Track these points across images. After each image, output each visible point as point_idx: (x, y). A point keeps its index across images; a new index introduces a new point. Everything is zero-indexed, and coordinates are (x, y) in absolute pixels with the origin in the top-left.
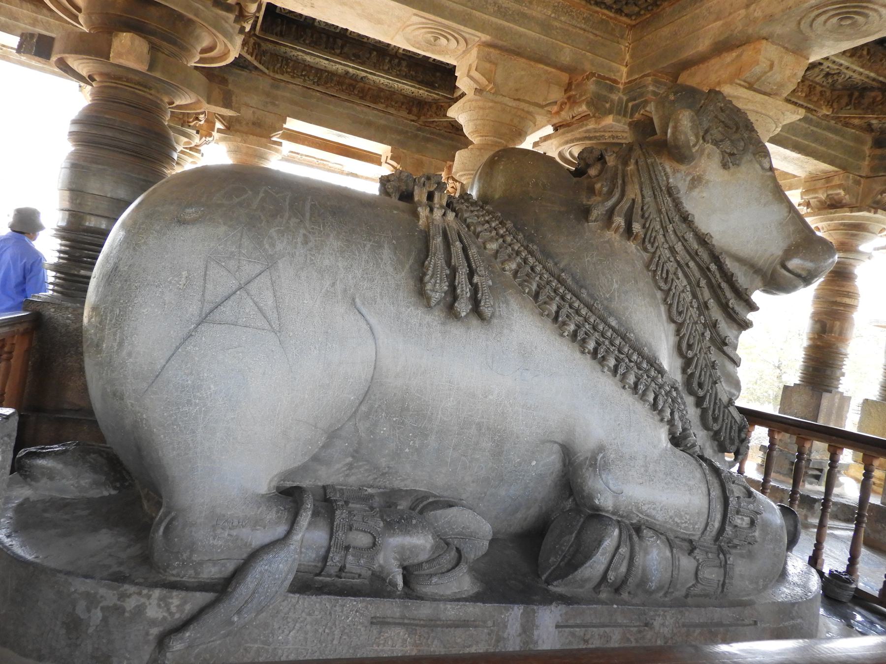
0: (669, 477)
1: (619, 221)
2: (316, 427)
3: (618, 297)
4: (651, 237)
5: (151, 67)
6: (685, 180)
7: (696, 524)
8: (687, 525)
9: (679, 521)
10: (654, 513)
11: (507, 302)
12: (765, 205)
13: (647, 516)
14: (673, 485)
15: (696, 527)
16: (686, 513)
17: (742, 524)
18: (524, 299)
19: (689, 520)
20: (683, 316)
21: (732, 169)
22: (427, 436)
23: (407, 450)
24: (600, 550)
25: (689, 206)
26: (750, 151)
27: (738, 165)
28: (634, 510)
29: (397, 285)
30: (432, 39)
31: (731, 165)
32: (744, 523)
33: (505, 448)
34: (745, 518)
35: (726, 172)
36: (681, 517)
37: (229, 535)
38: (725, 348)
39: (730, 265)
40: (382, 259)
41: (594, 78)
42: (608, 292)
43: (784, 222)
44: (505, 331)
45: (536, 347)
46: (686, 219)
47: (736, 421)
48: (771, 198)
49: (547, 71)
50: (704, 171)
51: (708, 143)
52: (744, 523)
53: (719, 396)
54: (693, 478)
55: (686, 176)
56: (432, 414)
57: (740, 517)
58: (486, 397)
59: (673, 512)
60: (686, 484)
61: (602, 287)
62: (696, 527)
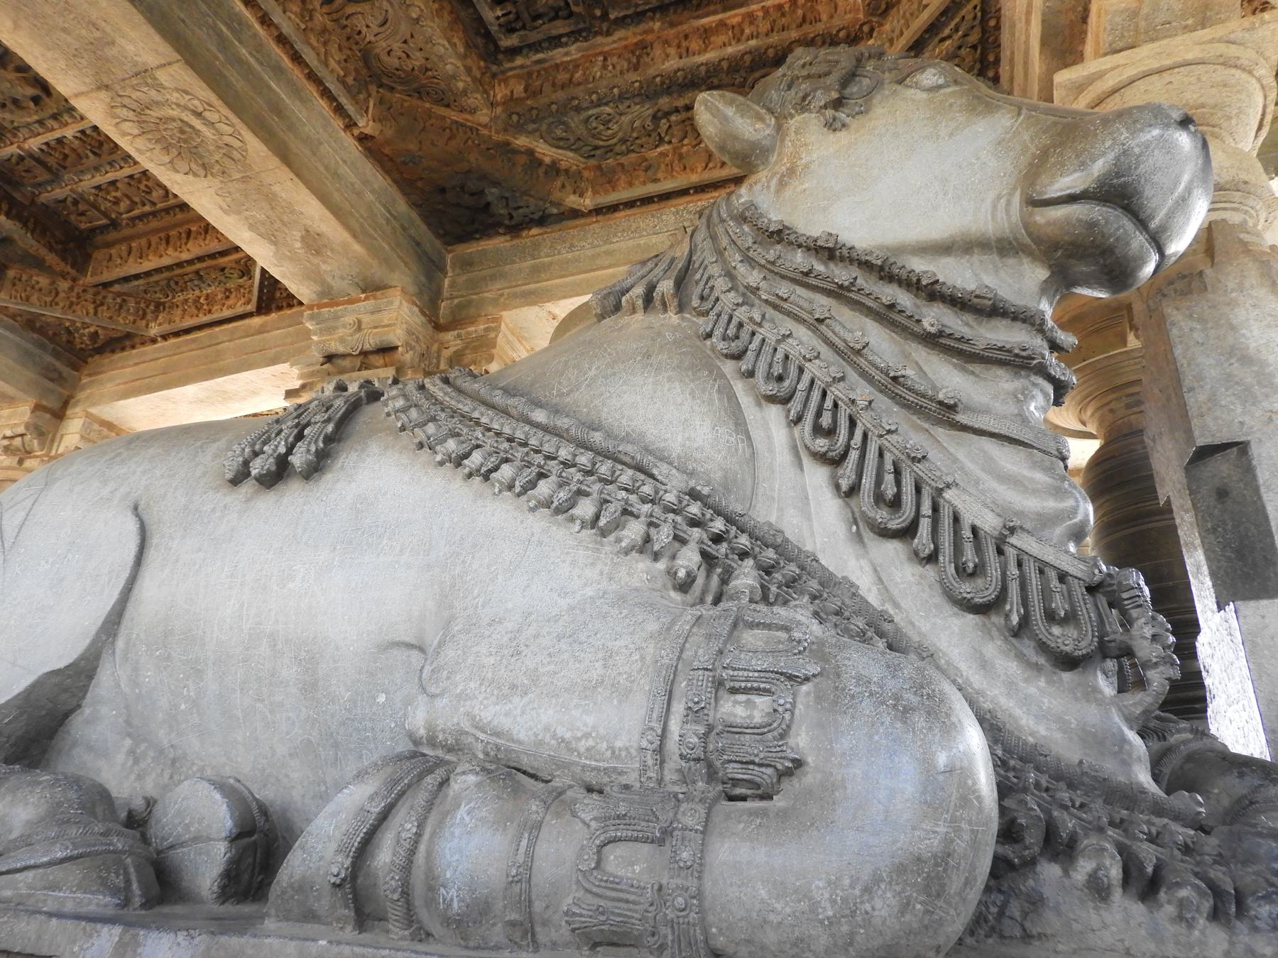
6: (768, 187)
8: (591, 743)
9: (568, 735)
12: (951, 135)
13: (497, 734)
14: (566, 656)
15: (618, 744)
17: (751, 717)
19: (594, 727)
25: (775, 215)
27: (867, 112)
29: (204, 474)
31: (848, 120)
34: (759, 700)
35: (842, 135)
38: (961, 418)
39: (919, 265)
43: (1008, 136)
45: (386, 493)
46: (779, 235)
47: (1063, 577)
51: (792, 116)
53: (968, 519)
56: (204, 633)
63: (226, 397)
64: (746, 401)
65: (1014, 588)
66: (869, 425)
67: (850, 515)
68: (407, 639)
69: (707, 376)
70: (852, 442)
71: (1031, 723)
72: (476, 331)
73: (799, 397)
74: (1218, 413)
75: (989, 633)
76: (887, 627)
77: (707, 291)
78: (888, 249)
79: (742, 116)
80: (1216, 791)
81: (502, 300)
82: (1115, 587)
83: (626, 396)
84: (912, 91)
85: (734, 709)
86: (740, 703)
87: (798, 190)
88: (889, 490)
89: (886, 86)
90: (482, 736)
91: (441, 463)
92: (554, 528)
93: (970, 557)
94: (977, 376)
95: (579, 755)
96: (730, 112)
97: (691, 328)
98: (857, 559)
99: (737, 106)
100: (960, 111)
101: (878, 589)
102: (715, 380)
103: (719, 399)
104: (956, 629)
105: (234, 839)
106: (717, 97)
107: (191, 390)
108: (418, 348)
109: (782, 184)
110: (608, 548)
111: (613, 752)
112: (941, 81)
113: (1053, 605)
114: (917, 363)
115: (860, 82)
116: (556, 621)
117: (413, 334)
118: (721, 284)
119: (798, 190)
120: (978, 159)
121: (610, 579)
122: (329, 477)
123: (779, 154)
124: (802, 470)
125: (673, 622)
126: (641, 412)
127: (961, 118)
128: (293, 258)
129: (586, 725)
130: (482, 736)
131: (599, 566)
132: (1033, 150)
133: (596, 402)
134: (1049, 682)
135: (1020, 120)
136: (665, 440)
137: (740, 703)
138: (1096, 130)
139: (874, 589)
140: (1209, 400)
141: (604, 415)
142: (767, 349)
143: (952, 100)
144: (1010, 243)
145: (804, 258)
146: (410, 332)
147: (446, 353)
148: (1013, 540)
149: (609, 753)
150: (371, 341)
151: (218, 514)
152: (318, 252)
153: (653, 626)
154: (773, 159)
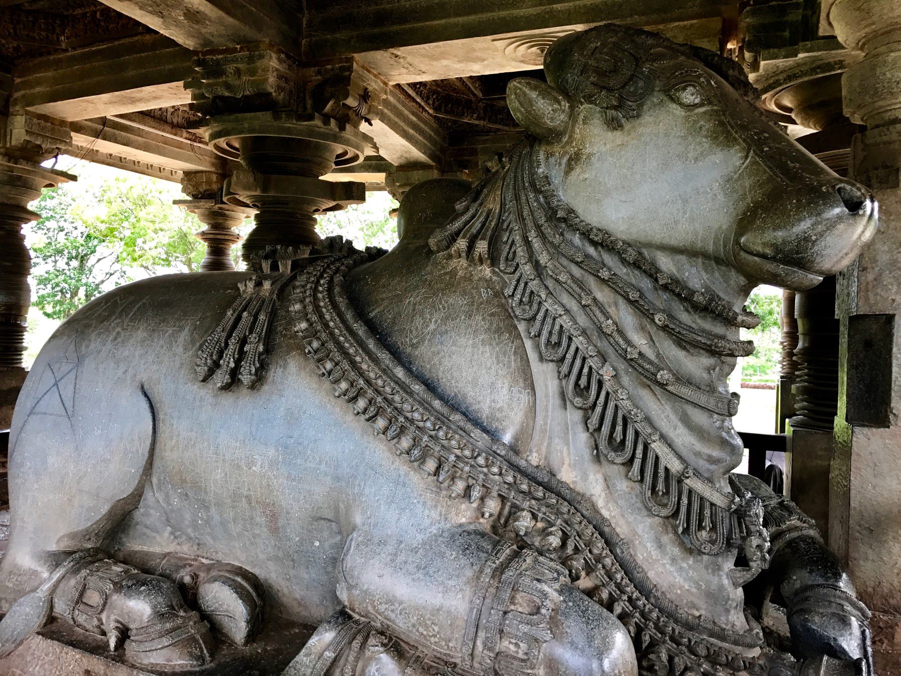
0: (421, 571)
1: (462, 243)
2: (97, 496)
3: (429, 340)
4: (508, 253)
5: (265, 189)
6: (560, 164)
7: (450, 641)
8: (436, 640)
9: (425, 633)
10: (392, 616)
11: (285, 367)
12: (696, 159)
13: (388, 620)
16: (433, 623)
17: (517, 652)
18: (306, 359)
19: (438, 633)
20: (561, 351)
21: (627, 126)
22: (207, 508)
23: (200, 522)
24: (303, 651)
26: (657, 89)
27: (638, 116)
28: (370, 608)
29: (182, 364)
30: (539, 51)
31: (623, 121)
32: (520, 652)
33: (280, 525)
35: (618, 133)
36: (427, 627)
37: (16, 580)
40: (176, 342)
41: (748, 8)
42: (416, 337)
43: (736, 176)
44: (274, 398)
45: (304, 412)
48: (706, 145)
49: (685, 27)
50: (583, 143)
51: (582, 104)
52: (520, 652)
53: (663, 463)
54: (458, 576)
55: (560, 158)
57: (513, 641)
58: (250, 468)
59: (415, 618)
60: (442, 583)
61: (411, 332)
62: (451, 644)
63: (133, 101)
64: (532, 356)
65: (683, 510)
66: (610, 391)
67: (593, 443)
68: (329, 518)
69: (508, 339)
70: (598, 402)
71: (681, 581)
72: (333, 69)
73: (568, 361)
74: (879, 291)
75: (666, 530)
76: (606, 529)
77: (511, 255)
78: (640, 243)
79: (543, 98)
80: (795, 578)
81: (352, 43)
82: (743, 512)
83: (454, 357)
84: (674, 106)
85: (507, 645)
86: (512, 643)
87: (581, 178)
88: (618, 436)
89: (656, 93)
90: (380, 617)
91: (339, 397)
92: (412, 473)
93: (661, 486)
94: (688, 351)
95: (431, 643)
96: (534, 95)
97: (498, 283)
98: (595, 475)
99: (540, 91)
100: (706, 137)
101: (606, 494)
102: (513, 342)
103: (515, 360)
104: (648, 524)
105: (248, 622)
106: (525, 84)
107: (105, 97)
108: (287, 87)
109: (569, 168)
110: (444, 492)
111: (448, 647)
112: (697, 101)
113: (704, 524)
114: (649, 333)
115: (636, 82)
116: (416, 553)
117: (283, 76)
118: (521, 252)
119: (581, 178)
120: (711, 189)
121: (446, 519)
122: (266, 388)
123: (570, 137)
124: (566, 409)
125: (481, 571)
126: (464, 374)
127: (706, 143)
128: (177, 24)
129: (434, 630)
130: (380, 617)
131: (439, 508)
132: (749, 200)
133: (436, 360)
134: (695, 561)
135: (746, 164)
136: (479, 402)
137: (512, 643)
138: (791, 210)
139: (603, 495)
140: (875, 279)
141: (441, 375)
142: (549, 320)
143: (702, 123)
144: (723, 261)
145: (580, 239)
146: (280, 77)
147: (310, 86)
148: (687, 481)
149: (446, 647)
150: (250, 89)
151: (198, 404)
152: (198, 22)
153: (469, 573)
154: (565, 139)
